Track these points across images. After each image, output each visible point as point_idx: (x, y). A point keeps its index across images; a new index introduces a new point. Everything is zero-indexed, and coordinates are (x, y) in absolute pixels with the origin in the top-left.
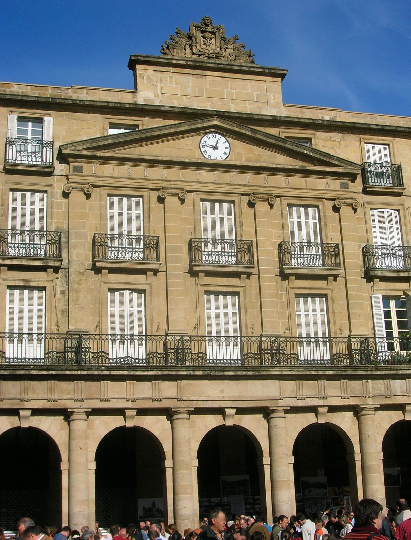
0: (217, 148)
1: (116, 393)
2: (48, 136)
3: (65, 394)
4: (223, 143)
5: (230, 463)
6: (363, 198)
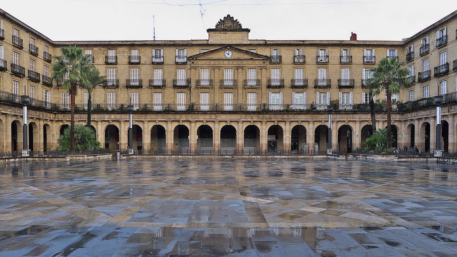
0: (229, 54)
1: (201, 117)
3: (190, 117)
4: (230, 53)
5: (228, 133)
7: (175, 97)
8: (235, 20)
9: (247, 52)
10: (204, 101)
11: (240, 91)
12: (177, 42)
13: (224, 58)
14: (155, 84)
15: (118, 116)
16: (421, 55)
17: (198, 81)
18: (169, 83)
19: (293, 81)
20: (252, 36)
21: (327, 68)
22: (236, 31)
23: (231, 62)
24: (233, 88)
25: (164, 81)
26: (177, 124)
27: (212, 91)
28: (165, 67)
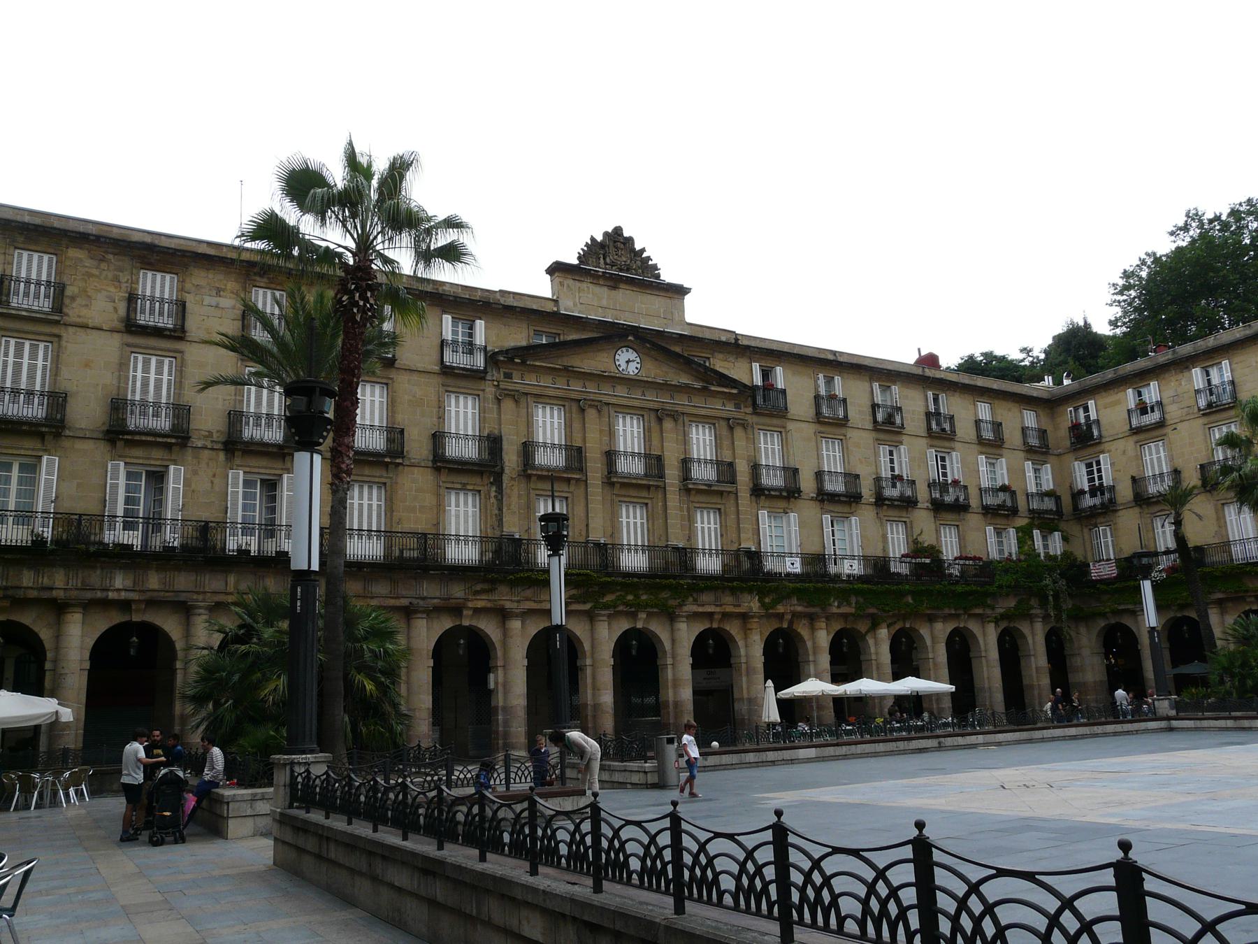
0: (627, 361)
2: (480, 339)
4: (631, 355)
6: (752, 419)
7: (440, 508)
8: (638, 247)
11: (674, 499)
12: (447, 288)
15: (183, 581)
17: (528, 449)
18: (418, 446)
20: (700, 312)
26: (447, 623)
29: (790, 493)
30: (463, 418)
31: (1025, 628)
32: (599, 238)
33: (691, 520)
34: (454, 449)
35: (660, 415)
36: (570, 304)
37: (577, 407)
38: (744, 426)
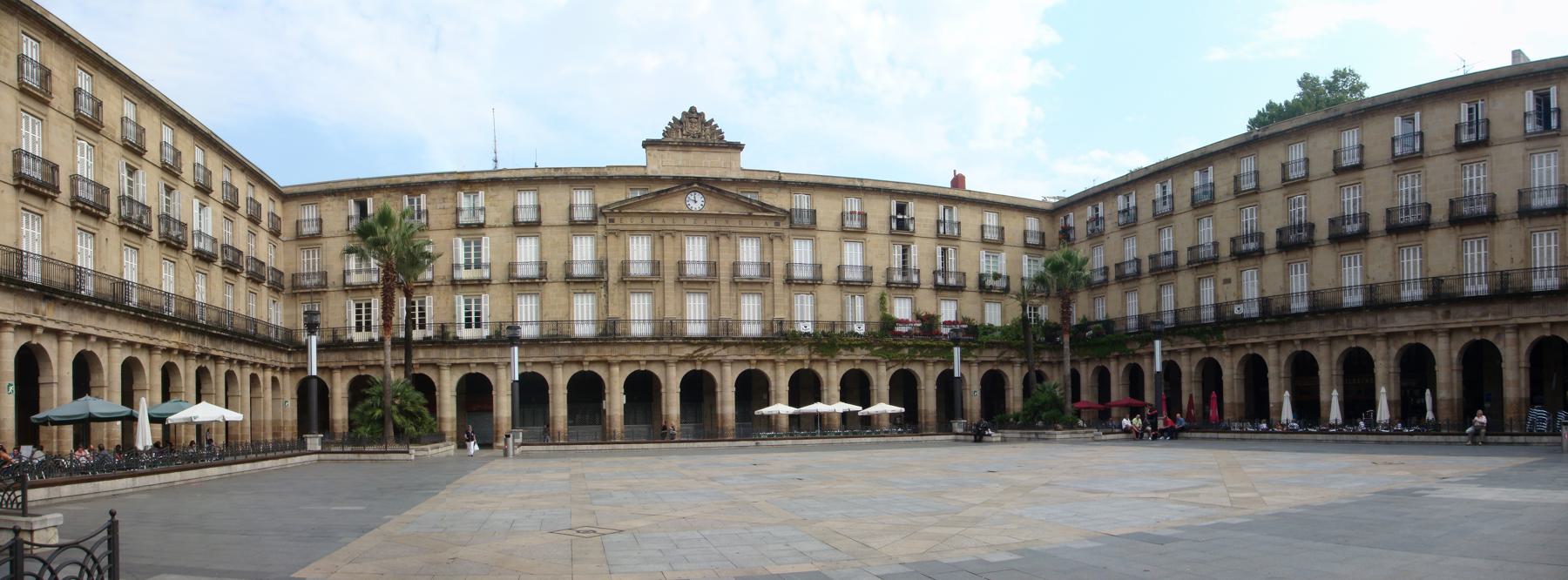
0: (696, 202)
1: (635, 353)
3: (608, 353)
4: (699, 198)
6: (787, 233)
7: (570, 305)
8: (707, 119)
9: (737, 200)
10: (640, 313)
13: (686, 210)
14: (522, 272)
16: (1158, 217)
17: (625, 266)
18: (555, 270)
19: (840, 268)
20: (752, 161)
21: (813, 239)
22: (713, 146)
23: (701, 222)
24: (705, 283)
25: (542, 265)
26: (575, 370)
27: (658, 288)
28: (546, 232)
29: (815, 282)
30: (584, 251)
31: (1006, 370)
32: (679, 117)
33: (738, 302)
34: (578, 271)
35: (717, 235)
36: (655, 167)
37: (659, 235)
38: (781, 237)
